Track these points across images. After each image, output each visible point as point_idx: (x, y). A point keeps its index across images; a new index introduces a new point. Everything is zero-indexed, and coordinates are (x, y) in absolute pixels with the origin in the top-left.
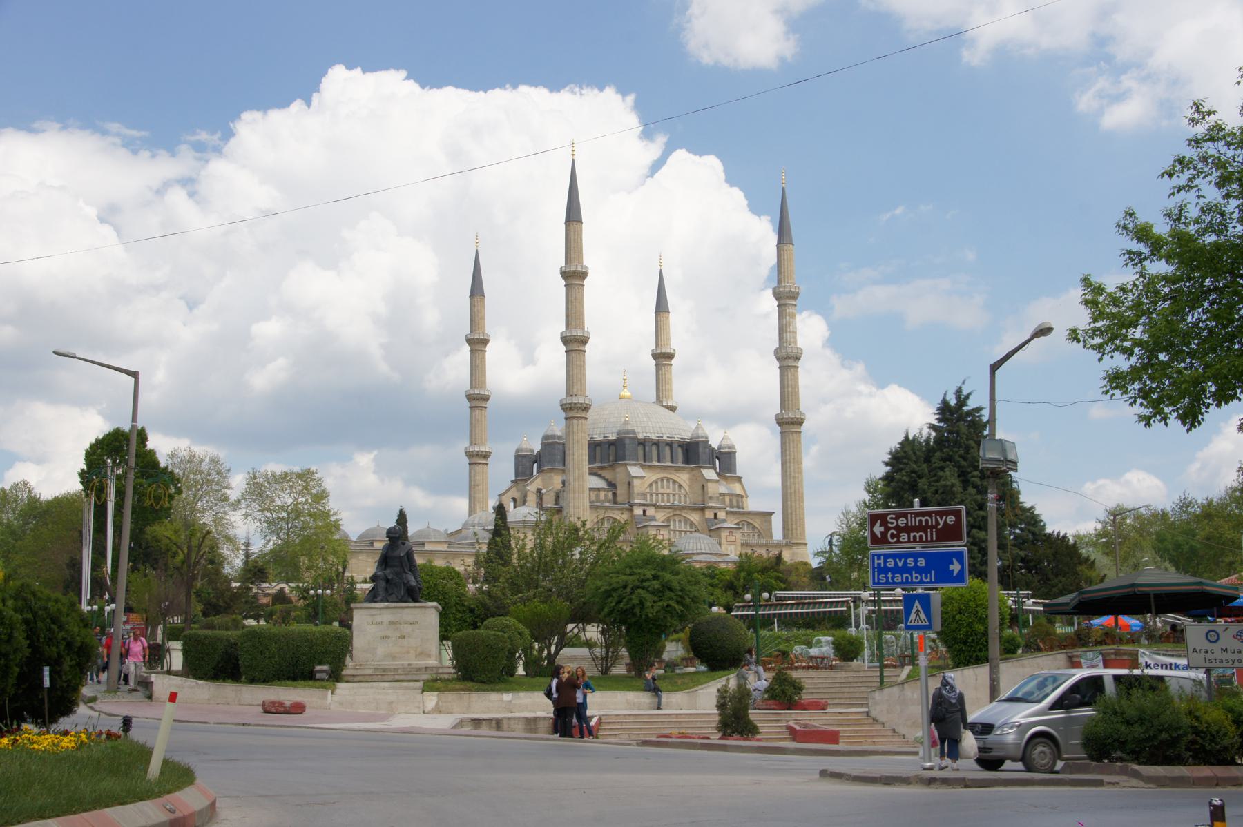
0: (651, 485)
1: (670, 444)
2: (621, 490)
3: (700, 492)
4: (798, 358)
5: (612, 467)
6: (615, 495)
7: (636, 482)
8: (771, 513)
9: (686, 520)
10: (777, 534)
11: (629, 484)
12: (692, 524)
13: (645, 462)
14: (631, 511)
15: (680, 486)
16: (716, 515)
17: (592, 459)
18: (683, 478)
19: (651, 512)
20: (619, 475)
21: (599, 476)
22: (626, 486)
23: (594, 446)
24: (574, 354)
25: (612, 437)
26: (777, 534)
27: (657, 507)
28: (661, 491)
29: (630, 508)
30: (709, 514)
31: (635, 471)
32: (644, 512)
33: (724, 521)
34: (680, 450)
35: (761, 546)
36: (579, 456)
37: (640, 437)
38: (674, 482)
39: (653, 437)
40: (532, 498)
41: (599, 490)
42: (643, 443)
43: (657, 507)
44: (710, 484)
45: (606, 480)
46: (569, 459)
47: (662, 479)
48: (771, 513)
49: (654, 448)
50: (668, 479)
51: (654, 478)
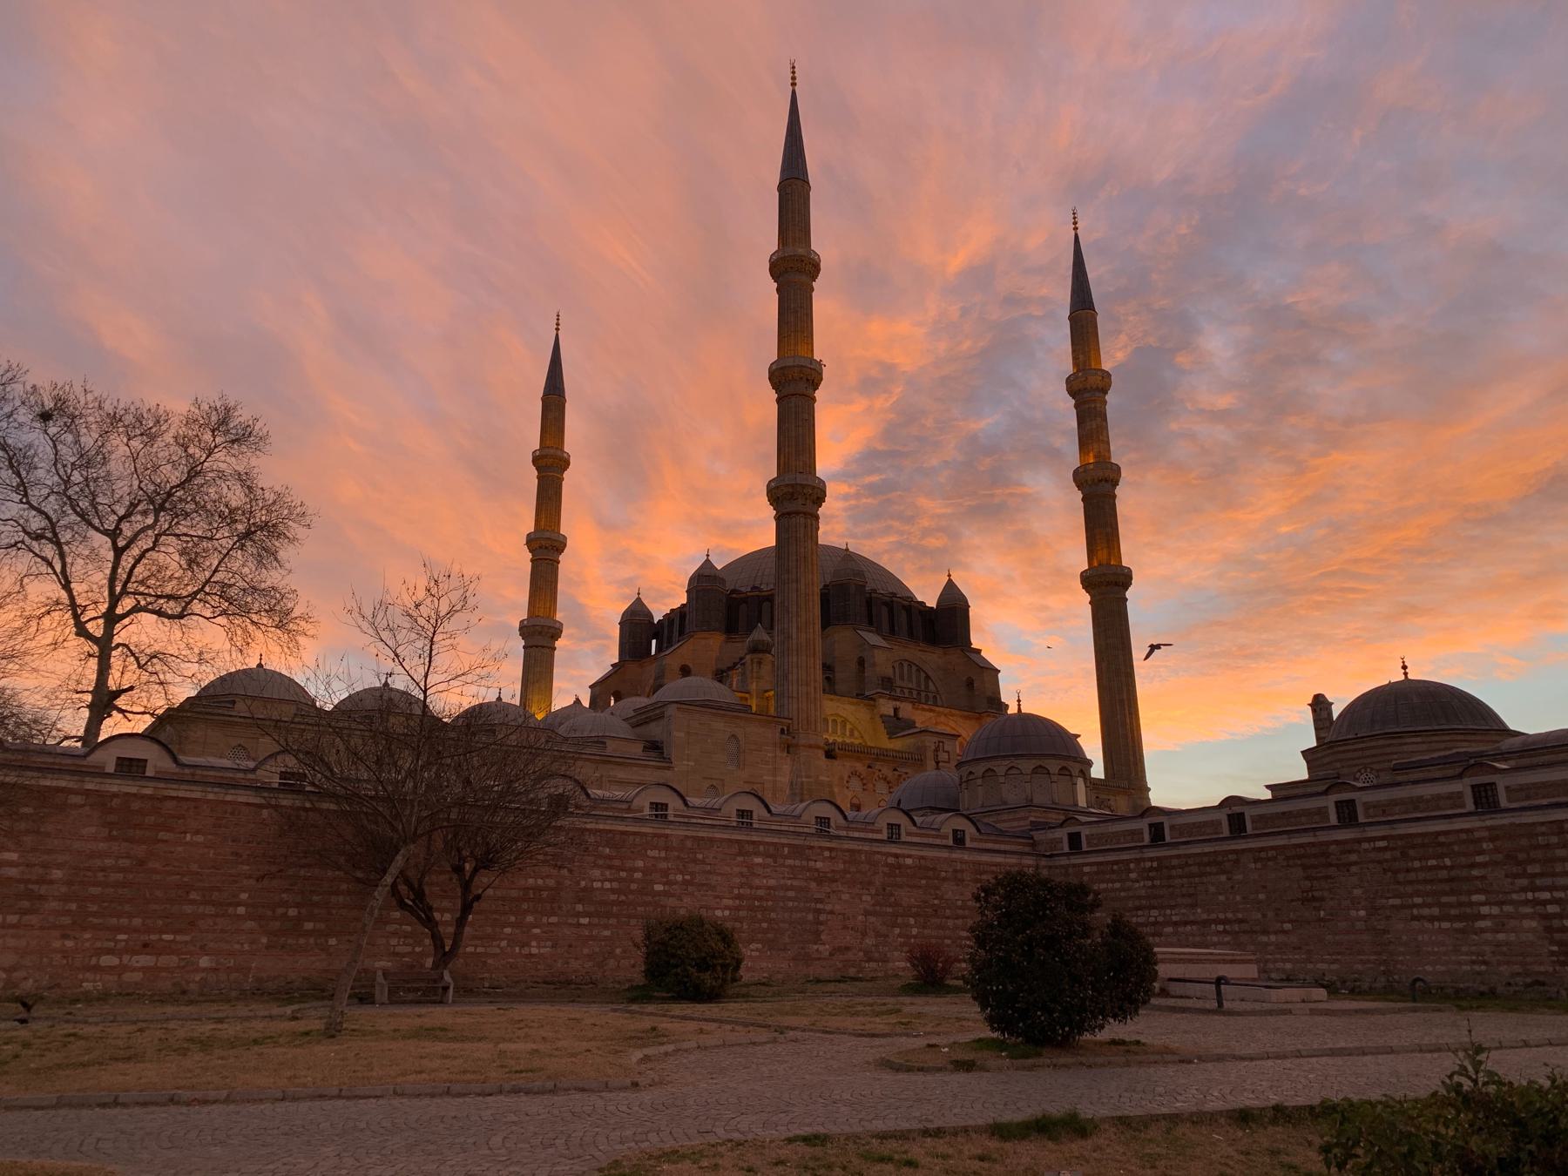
7: (880, 657)
15: (928, 677)
38: (919, 669)
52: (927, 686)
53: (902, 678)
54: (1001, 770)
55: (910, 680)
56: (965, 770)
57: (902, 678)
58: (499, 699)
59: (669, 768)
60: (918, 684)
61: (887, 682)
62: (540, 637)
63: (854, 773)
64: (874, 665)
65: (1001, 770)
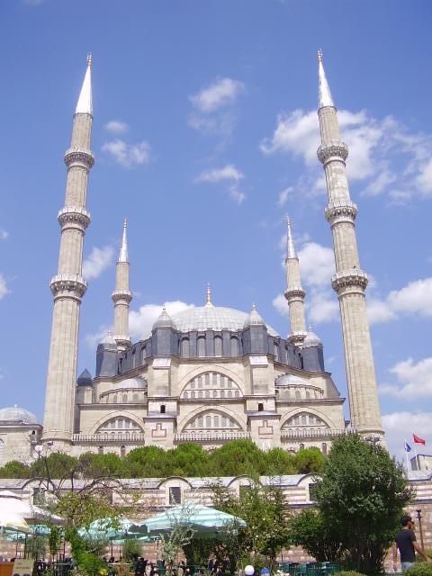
0: (192, 380)
9: (225, 415)
12: (232, 420)
14: (146, 407)
15: (230, 380)
18: (235, 370)
19: (171, 406)
27: (180, 402)
28: (205, 387)
30: (252, 405)
32: (163, 409)
35: (313, 439)
38: (223, 375)
41: (127, 390)
44: (255, 371)
47: (207, 373)
50: (215, 373)
53: (207, 383)
55: (215, 382)
57: (207, 383)
60: (222, 384)
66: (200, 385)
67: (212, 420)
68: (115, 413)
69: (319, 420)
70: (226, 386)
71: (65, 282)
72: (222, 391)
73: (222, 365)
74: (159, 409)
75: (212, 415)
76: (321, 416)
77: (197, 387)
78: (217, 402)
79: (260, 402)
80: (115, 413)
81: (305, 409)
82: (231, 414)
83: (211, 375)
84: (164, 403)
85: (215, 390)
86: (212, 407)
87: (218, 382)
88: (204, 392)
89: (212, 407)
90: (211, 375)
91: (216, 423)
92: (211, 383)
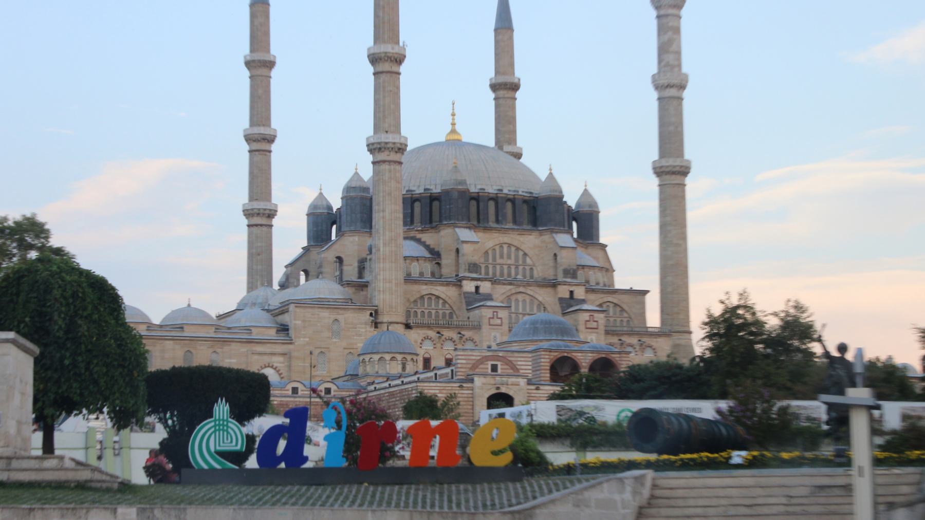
1: (513, 201)
2: (447, 260)
3: (551, 263)
4: (682, 87)
5: (435, 228)
6: (438, 264)
7: (466, 249)
8: (645, 292)
10: (653, 319)
11: (458, 251)
13: (479, 221)
14: (460, 286)
15: (525, 254)
16: (572, 292)
17: (409, 219)
19: (485, 287)
20: (442, 238)
21: (419, 241)
22: (453, 254)
23: (410, 201)
24: (383, 77)
25: (436, 190)
26: (653, 319)
28: (499, 261)
29: (458, 282)
31: (465, 234)
32: (477, 288)
33: (583, 301)
34: (525, 207)
36: (389, 214)
37: (473, 190)
38: (518, 249)
39: (491, 190)
40: (330, 269)
42: (476, 198)
43: (494, 282)
45: (427, 247)
46: (377, 217)
48: (645, 292)
49: (492, 205)
50: (510, 245)
51: (489, 244)
52: (524, 261)
53: (502, 257)
54: (367, 360)
55: (509, 257)
56: (361, 358)
57: (502, 257)
58: (189, 305)
59: (291, 343)
60: (517, 260)
61: (474, 267)
62: (260, 217)
63: (427, 338)
64: (463, 255)
65: (367, 360)
66: (494, 259)
67: (520, 304)
68: (425, 289)
69: (623, 310)
70: (520, 262)
71: (394, 143)
72: (517, 267)
73: (518, 237)
74: (473, 290)
75: (520, 297)
76: (625, 307)
77: (490, 261)
78: (528, 284)
79: (571, 289)
80: (425, 289)
81: (610, 299)
82: (540, 299)
83: (505, 247)
84: (479, 283)
85: (509, 266)
86: (521, 289)
87: (513, 256)
88: (498, 267)
89: (521, 289)
90: (505, 247)
91: (524, 309)
92: (505, 256)
